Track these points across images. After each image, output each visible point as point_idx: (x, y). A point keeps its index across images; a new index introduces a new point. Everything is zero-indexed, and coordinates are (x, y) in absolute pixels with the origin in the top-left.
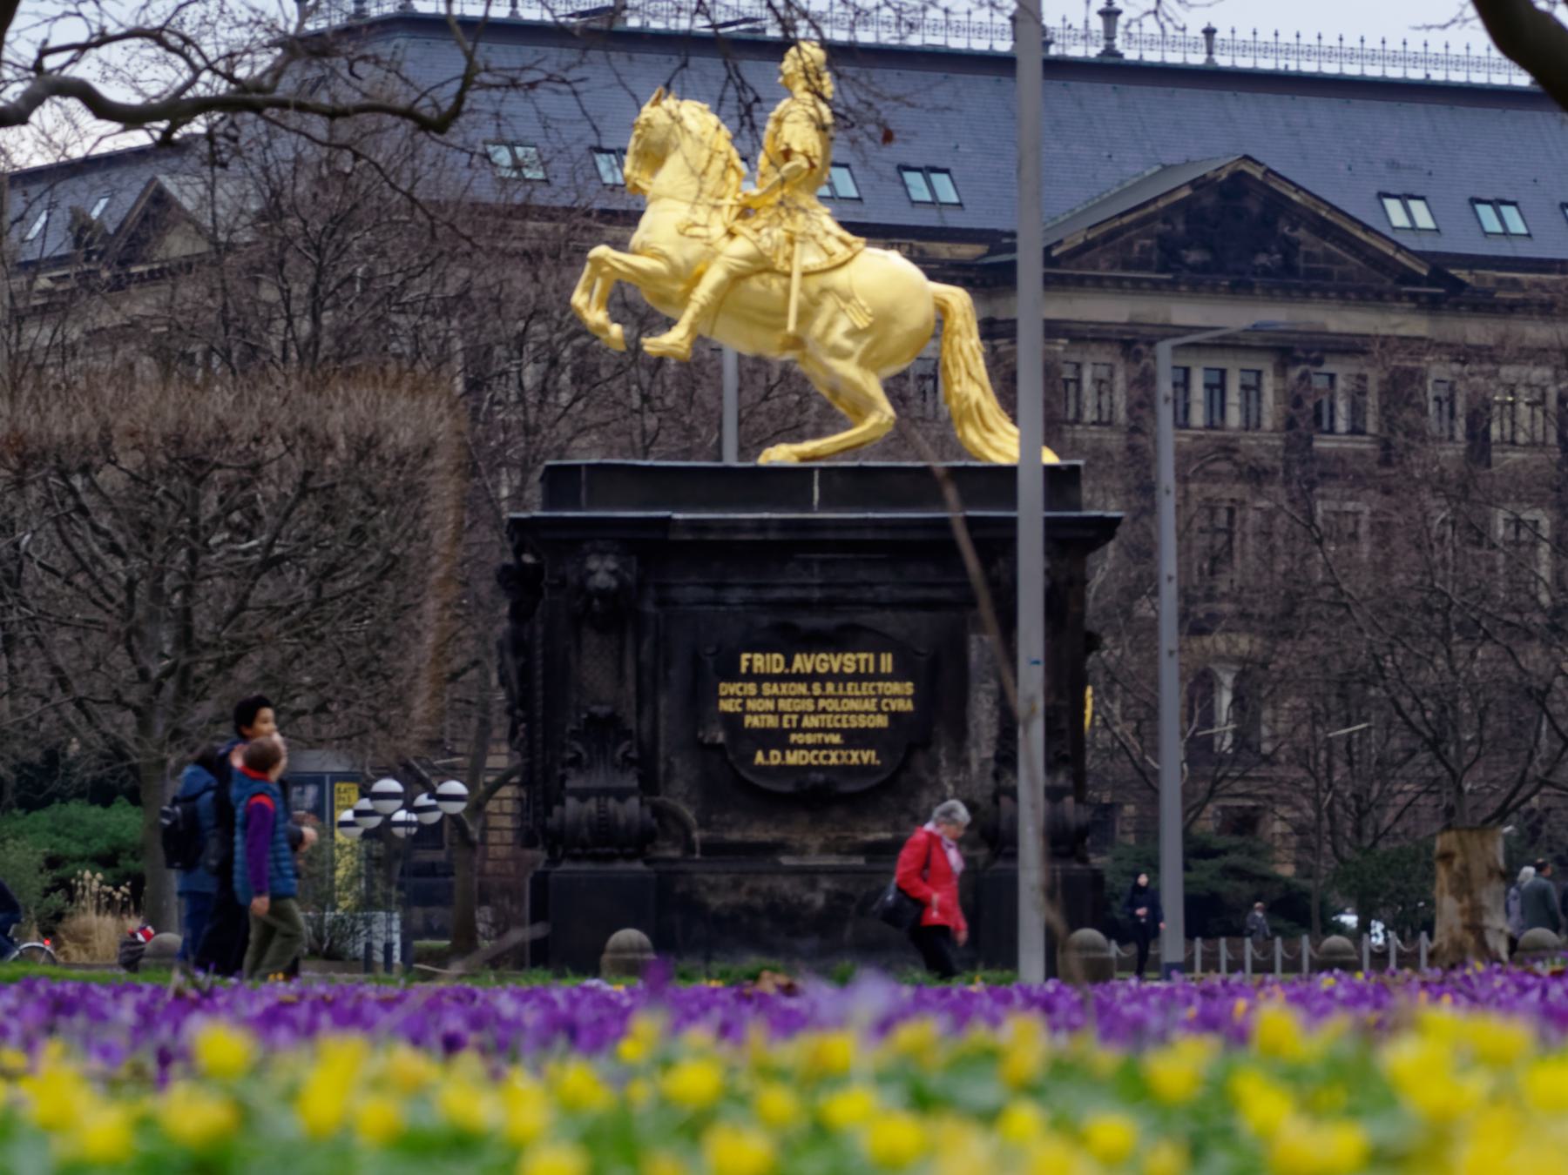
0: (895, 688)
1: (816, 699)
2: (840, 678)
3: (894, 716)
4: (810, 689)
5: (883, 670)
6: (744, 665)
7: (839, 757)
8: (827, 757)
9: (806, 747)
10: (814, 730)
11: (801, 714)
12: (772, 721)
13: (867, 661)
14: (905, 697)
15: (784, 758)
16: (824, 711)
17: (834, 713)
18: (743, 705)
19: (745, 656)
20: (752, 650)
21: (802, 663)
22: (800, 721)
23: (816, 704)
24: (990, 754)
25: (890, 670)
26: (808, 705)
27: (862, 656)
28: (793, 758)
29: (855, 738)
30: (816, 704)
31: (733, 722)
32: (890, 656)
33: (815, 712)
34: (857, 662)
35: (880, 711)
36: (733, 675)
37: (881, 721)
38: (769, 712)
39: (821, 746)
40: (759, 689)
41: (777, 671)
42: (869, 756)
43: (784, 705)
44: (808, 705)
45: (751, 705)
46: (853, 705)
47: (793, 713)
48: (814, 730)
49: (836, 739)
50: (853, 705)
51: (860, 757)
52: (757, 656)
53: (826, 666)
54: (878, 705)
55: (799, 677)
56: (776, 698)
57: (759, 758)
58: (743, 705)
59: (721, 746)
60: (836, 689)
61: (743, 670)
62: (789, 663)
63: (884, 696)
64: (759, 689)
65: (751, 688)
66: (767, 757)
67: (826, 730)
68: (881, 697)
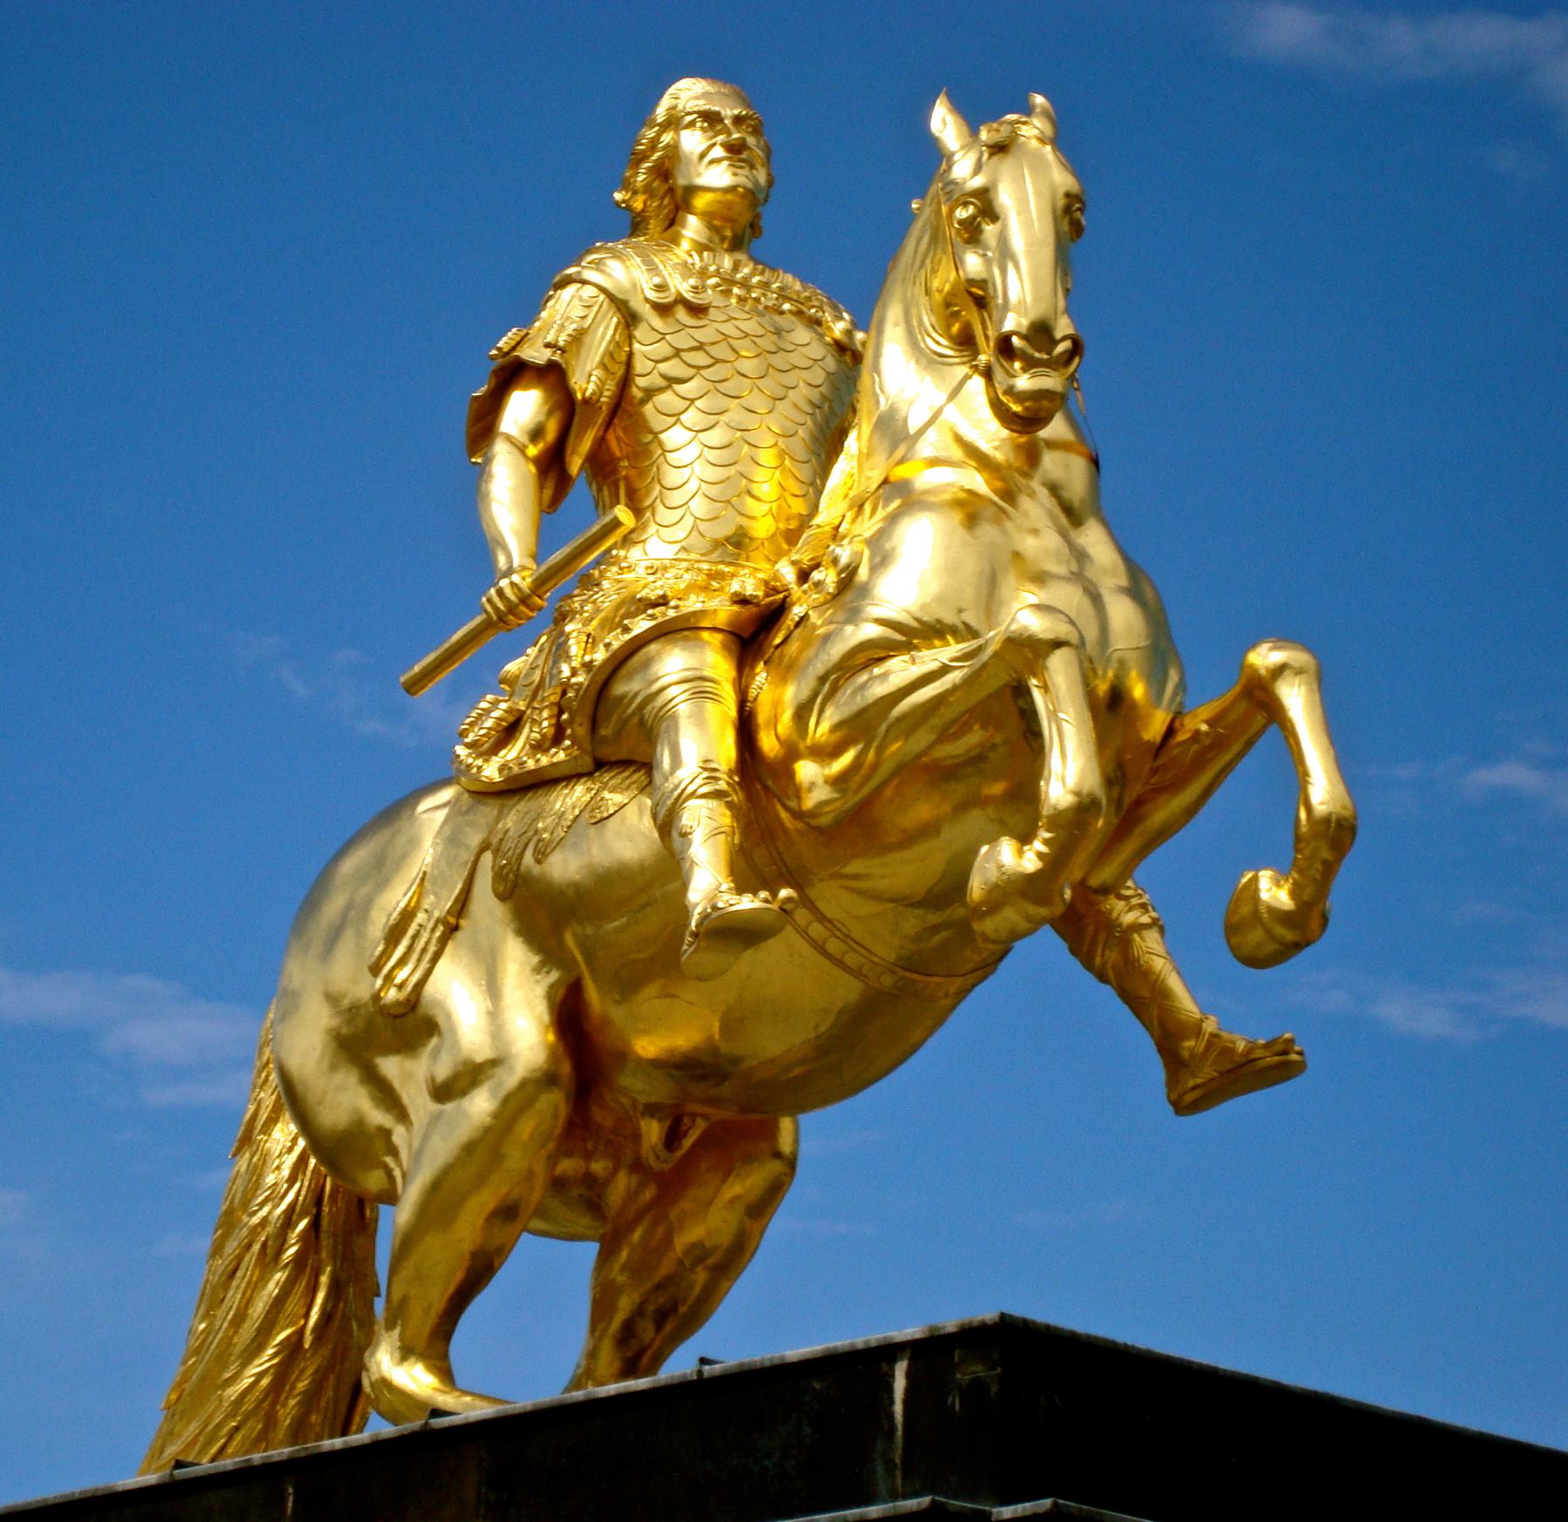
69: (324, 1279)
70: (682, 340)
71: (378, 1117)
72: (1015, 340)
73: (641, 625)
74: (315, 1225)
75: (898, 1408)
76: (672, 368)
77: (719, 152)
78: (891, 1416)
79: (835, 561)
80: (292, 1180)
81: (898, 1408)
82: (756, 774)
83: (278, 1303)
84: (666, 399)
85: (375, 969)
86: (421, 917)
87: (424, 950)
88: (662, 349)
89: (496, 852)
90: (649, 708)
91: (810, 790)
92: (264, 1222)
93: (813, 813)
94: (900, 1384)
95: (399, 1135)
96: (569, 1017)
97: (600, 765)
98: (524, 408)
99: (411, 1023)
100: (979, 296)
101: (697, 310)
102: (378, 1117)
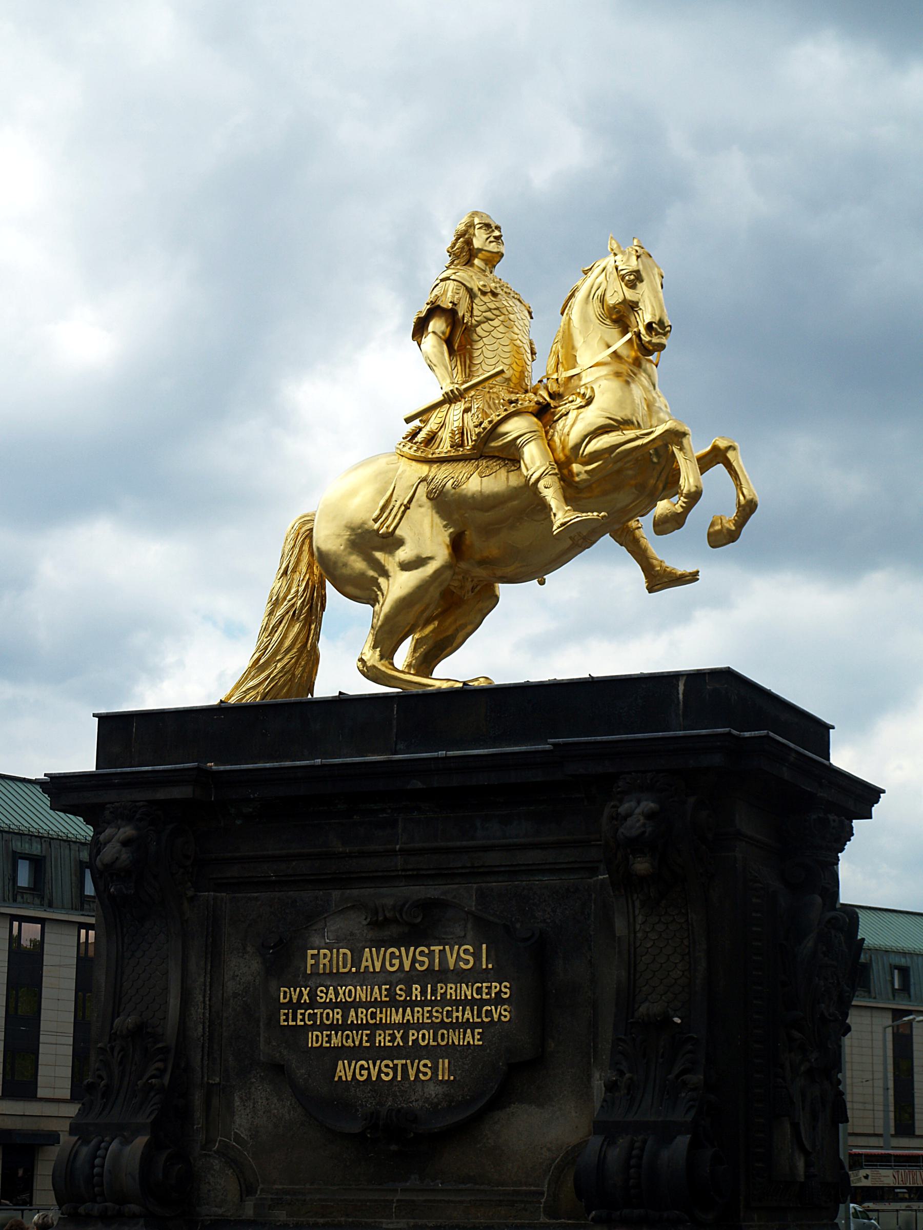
19: (310, 952)
21: (372, 960)
27: (437, 949)
34: (431, 954)
36: (298, 979)
41: (342, 970)
53: (396, 962)
62: (356, 962)
69: (313, 626)
70: (492, 306)
71: (371, 573)
72: (654, 325)
73: (511, 409)
74: (311, 607)
75: (681, 696)
76: (488, 314)
77: (492, 239)
78: (678, 698)
79: (584, 395)
80: (304, 591)
81: (681, 696)
82: (562, 469)
83: (298, 634)
84: (485, 326)
85: (376, 520)
86: (392, 503)
87: (396, 515)
88: (484, 308)
89: (429, 484)
90: (518, 441)
91: (578, 475)
92: (293, 605)
93: (577, 482)
94: (681, 688)
95: (382, 580)
96: (457, 545)
97: (481, 456)
98: (437, 325)
99: (392, 542)
100: (633, 306)
101: (495, 294)
102: (371, 573)
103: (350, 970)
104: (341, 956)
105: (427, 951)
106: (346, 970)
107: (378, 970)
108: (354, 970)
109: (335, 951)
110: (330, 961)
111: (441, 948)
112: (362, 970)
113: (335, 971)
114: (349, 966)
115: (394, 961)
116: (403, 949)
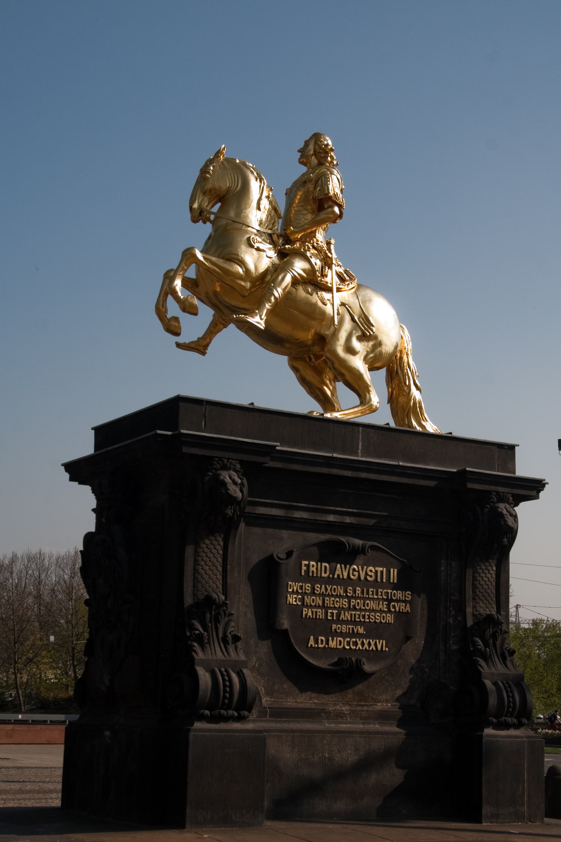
0: (399, 594)
1: (350, 598)
2: (365, 583)
3: (398, 615)
4: (346, 592)
5: (392, 581)
6: (304, 568)
7: (363, 644)
8: (356, 644)
9: (341, 634)
10: (347, 622)
11: (340, 609)
12: (320, 613)
13: (382, 572)
14: (405, 601)
15: (327, 643)
16: (355, 609)
17: (361, 610)
18: (302, 600)
20: (309, 560)
21: (341, 571)
22: (339, 615)
23: (349, 603)
24: (455, 647)
25: (395, 581)
26: (344, 603)
28: (332, 644)
29: (375, 630)
30: (349, 603)
31: (296, 611)
32: (396, 570)
33: (349, 609)
35: (389, 611)
36: (298, 578)
37: (390, 618)
38: (319, 607)
39: (353, 635)
40: (313, 589)
41: (323, 575)
42: (381, 644)
43: (328, 601)
44: (344, 603)
45: (308, 600)
46: (372, 605)
47: (335, 608)
48: (347, 622)
49: (361, 630)
50: (372, 605)
51: (376, 644)
52: (312, 563)
54: (388, 605)
55: (340, 581)
56: (323, 595)
57: (312, 642)
58: (302, 600)
59: (286, 631)
60: (362, 593)
61: (303, 574)
62: (333, 571)
63: (392, 600)
64: (313, 589)
65: (308, 587)
66: (316, 642)
67: (355, 623)
68: (389, 601)
103: (329, 576)
104: (323, 568)
105: (374, 571)
106: (326, 575)
107: (345, 577)
108: (331, 576)
109: (319, 564)
110: (317, 569)
111: (381, 569)
112: (336, 576)
113: (319, 575)
114: (328, 573)
115: (355, 573)
116: (360, 567)
